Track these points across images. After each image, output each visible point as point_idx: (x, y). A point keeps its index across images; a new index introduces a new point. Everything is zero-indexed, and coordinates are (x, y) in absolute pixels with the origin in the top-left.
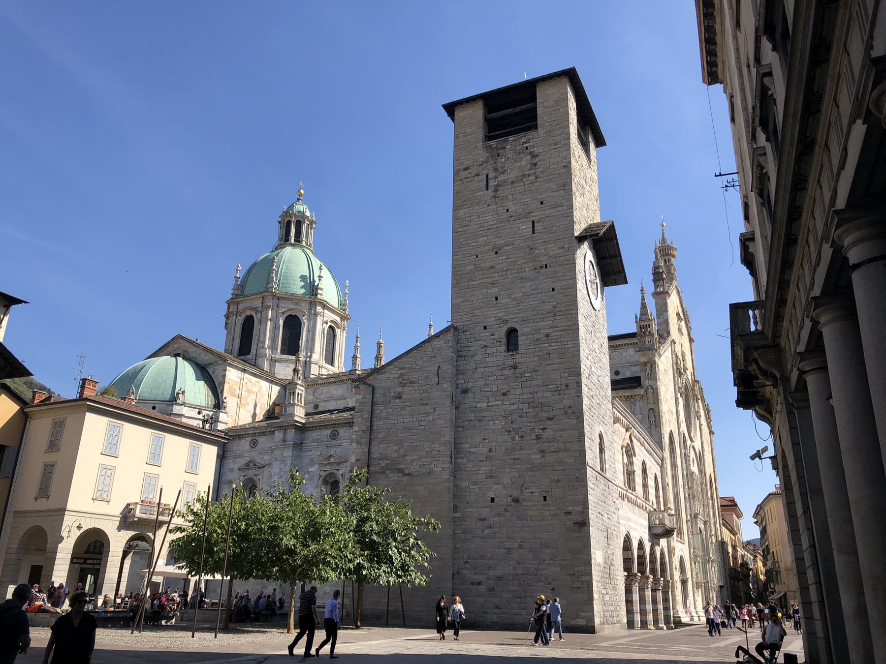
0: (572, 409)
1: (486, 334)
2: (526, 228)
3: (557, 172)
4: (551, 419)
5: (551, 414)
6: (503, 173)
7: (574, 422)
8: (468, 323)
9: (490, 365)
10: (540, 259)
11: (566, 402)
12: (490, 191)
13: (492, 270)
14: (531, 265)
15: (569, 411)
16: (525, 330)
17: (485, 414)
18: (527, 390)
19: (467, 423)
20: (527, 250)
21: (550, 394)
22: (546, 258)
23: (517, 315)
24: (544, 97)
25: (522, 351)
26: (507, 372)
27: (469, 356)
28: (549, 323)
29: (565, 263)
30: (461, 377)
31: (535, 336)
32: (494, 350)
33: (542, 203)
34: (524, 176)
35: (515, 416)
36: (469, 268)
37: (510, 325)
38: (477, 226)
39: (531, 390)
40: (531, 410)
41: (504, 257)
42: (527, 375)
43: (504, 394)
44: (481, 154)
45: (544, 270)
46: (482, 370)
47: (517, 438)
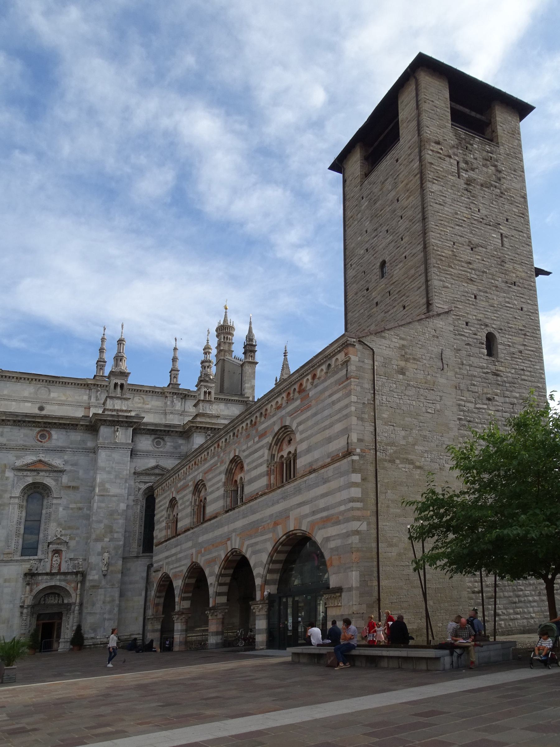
18: (507, 400)
23: (495, 322)
26: (490, 376)
37: (490, 330)
43: (489, 399)
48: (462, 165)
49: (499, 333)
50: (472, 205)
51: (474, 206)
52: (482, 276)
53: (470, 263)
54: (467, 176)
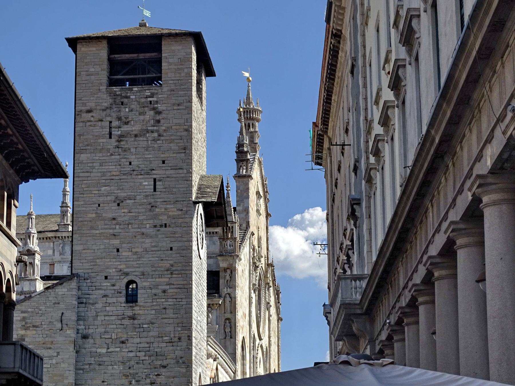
0: (183, 359)
1: (106, 284)
2: (148, 184)
3: (179, 134)
4: (164, 367)
5: (165, 363)
6: (127, 123)
7: (184, 370)
8: (90, 271)
9: (111, 314)
10: (160, 218)
11: (178, 353)
12: (113, 140)
13: (114, 222)
14: (151, 222)
15: (181, 361)
16: (145, 284)
17: (105, 359)
18: (144, 340)
19: (87, 367)
20: (149, 207)
21: (164, 345)
22: (166, 217)
23: (137, 269)
24: (169, 51)
25: (141, 304)
26: (126, 322)
27: (90, 303)
28: (167, 280)
29: (183, 225)
30: (81, 323)
31: (154, 291)
32: (114, 300)
33: (164, 162)
34: (148, 131)
35: (132, 363)
36: (90, 216)
37: (130, 278)
38: (99, 174)
39: (148, 340)
40: (147, 358)
41: (126, 211)
42: (145, 326)
43: (123, 342)
44: (106, 100)
45: (163, 229)
46: (103, 318)
47: (133, 382)
48: (115, 123)
49: (140, 278)
50: (123, 160)
51: (125, 160)
52: (128, 228)
53: (114, 219)
54: (120, 132)
